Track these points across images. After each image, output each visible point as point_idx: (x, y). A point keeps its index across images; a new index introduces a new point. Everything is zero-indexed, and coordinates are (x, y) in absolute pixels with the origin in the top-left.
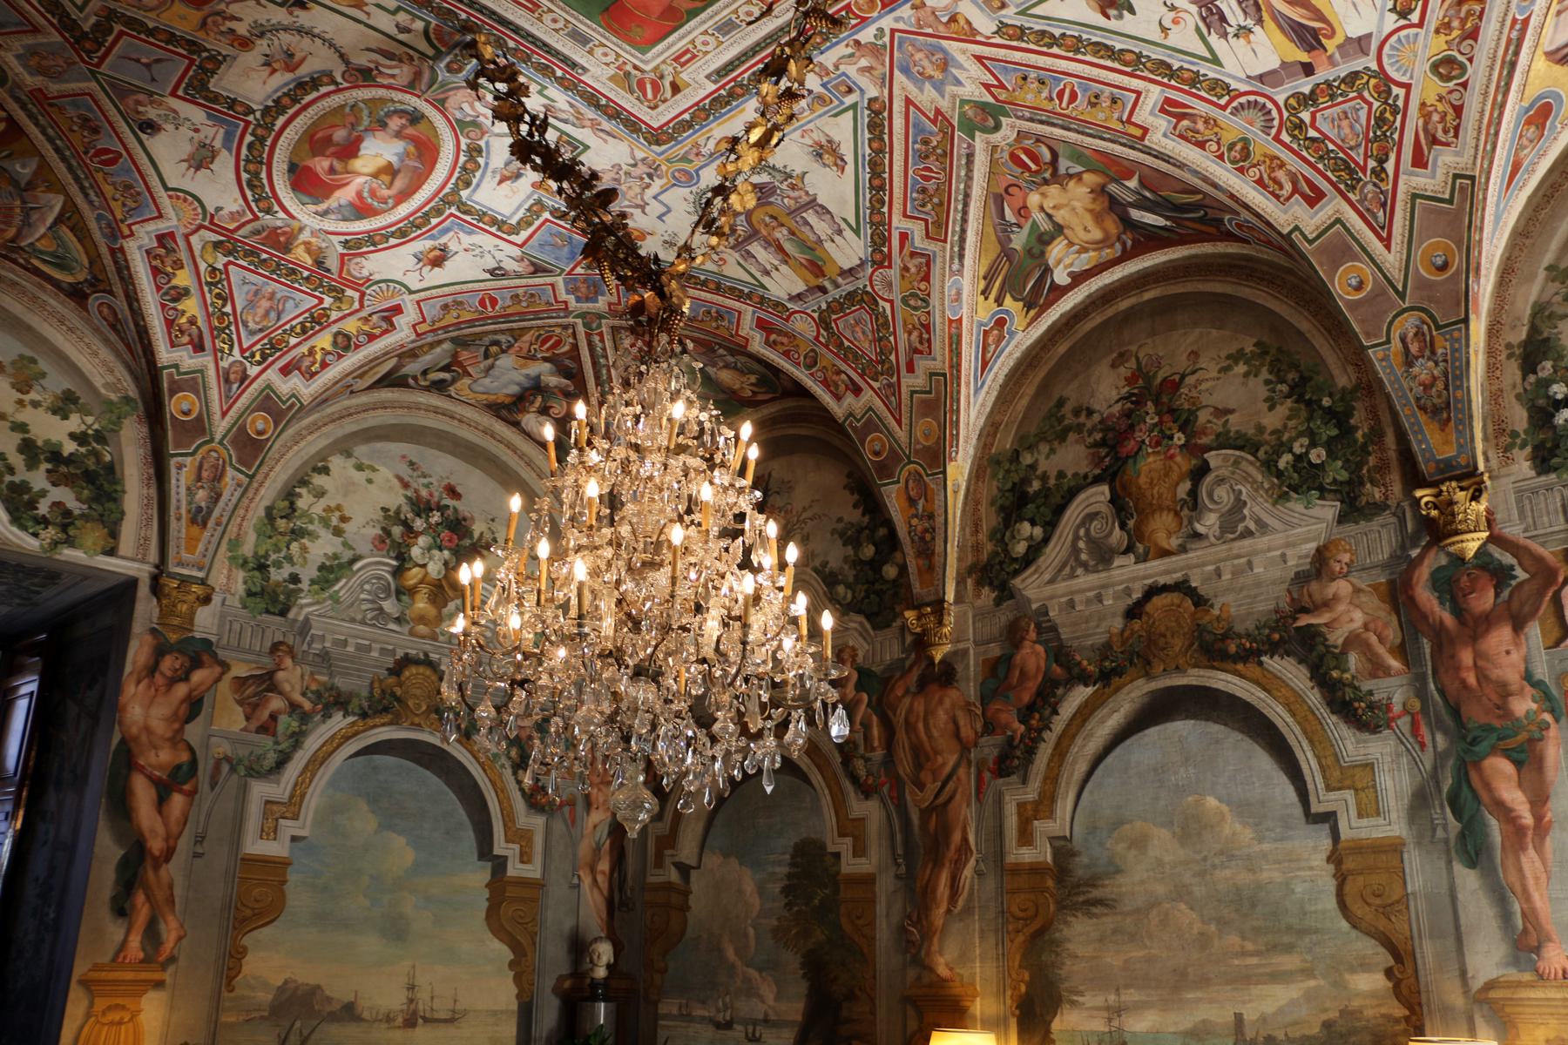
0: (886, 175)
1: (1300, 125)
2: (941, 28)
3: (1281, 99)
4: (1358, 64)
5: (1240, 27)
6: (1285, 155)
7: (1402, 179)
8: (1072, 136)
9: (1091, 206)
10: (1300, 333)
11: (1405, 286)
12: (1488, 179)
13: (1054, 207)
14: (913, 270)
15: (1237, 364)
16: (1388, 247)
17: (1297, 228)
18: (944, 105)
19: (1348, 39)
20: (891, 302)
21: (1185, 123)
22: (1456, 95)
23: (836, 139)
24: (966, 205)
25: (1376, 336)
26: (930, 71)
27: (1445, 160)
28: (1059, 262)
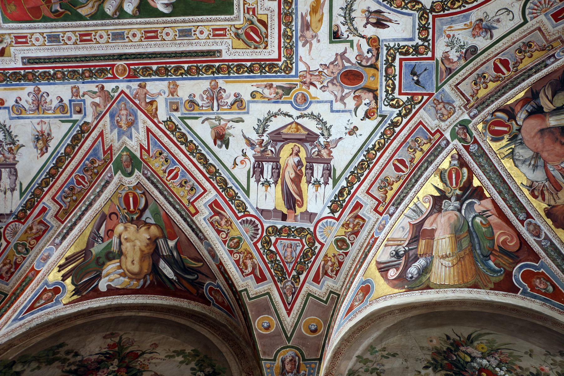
0: (61, 170)
1: (269, 242)
2: (143, 104)
3: (266, 226)
4: (306, 225)
5: (267, 181)
6: (255, 254)
7: (306, 285)
8: (161, 199)
9: (144, 248)
10: (220, 352)
11: (292, 335)
12: (344, 299)
13: (126, 239)
14: (34, 231)
15: (178, 356)
16: (289, 314)
17: (246, 290)
18: (116, 145)
19: (307, 211)
20: (8, 243)
21: (217, 217)
22: (341, 257)
23: (53, 135)
24: (87, 210)
25: (268, 355)
26: (123, 124)
27: (328, 283)
28: (108, 275)
